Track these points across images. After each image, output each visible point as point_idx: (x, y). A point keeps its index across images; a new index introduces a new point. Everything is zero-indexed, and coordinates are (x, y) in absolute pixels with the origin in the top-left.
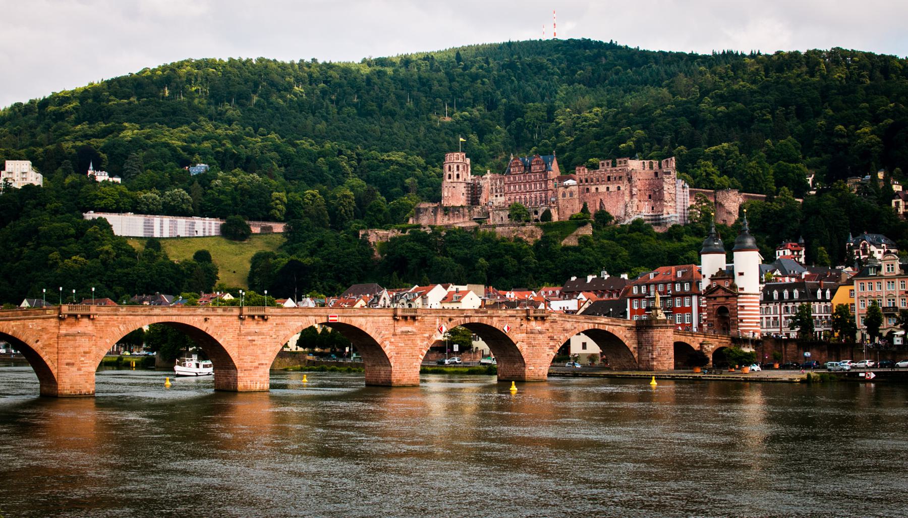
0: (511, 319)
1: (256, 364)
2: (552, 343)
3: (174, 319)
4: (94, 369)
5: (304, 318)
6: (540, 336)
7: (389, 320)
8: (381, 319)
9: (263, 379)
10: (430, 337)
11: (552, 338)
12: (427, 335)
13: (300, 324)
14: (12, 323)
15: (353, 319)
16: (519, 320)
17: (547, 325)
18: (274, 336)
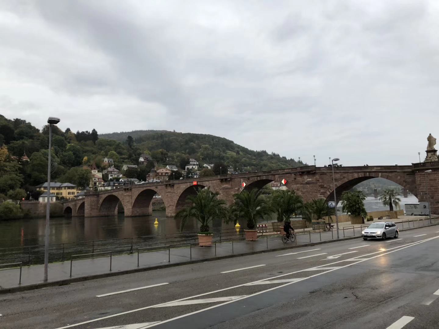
0: (287, 175)
1: (168, 205)
2: (322, 191)
3: (149, 188)
4: (131, 207)
5: (186, 184)
6: (308, 186)
7: (218, 182)
8: (215, 181)
9: (171, 212)
10: (239, 189)
11: (322, 187)
12: (237, 189)
13: (185, 187)
14: (117, 192)
15: (204, 183)
16: (293, 175)
17: (317, 177)
18: (176, 193)
